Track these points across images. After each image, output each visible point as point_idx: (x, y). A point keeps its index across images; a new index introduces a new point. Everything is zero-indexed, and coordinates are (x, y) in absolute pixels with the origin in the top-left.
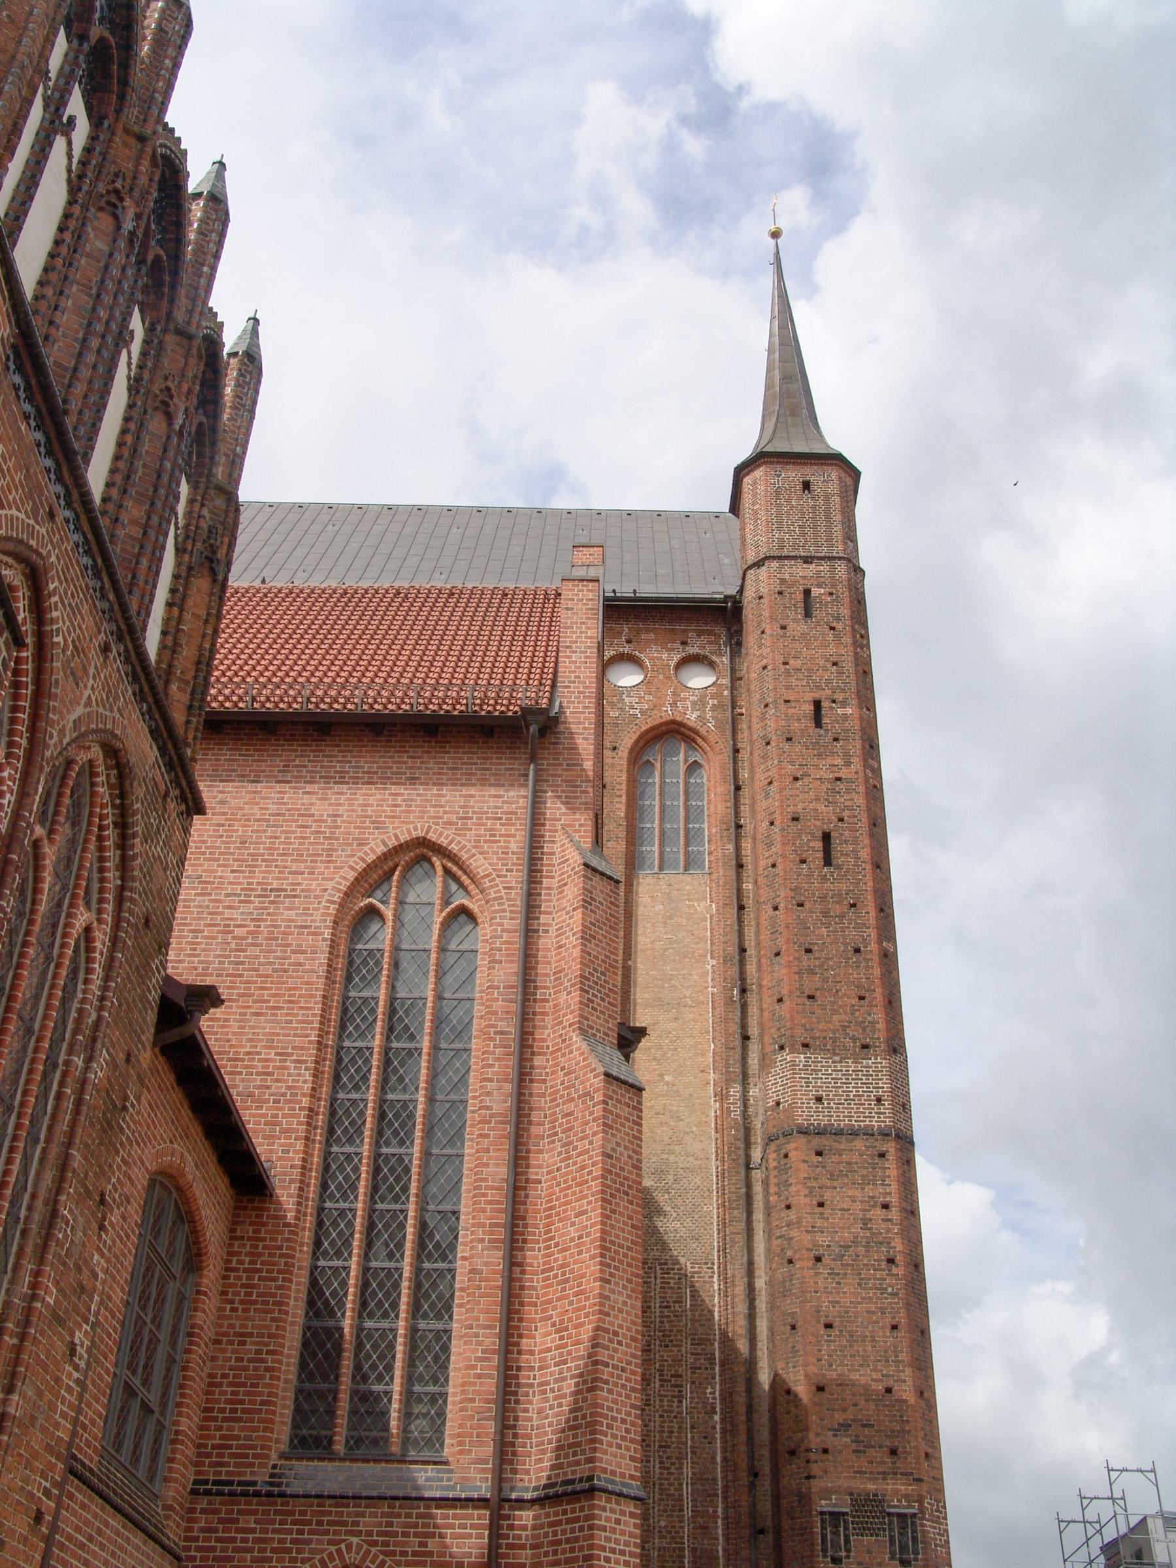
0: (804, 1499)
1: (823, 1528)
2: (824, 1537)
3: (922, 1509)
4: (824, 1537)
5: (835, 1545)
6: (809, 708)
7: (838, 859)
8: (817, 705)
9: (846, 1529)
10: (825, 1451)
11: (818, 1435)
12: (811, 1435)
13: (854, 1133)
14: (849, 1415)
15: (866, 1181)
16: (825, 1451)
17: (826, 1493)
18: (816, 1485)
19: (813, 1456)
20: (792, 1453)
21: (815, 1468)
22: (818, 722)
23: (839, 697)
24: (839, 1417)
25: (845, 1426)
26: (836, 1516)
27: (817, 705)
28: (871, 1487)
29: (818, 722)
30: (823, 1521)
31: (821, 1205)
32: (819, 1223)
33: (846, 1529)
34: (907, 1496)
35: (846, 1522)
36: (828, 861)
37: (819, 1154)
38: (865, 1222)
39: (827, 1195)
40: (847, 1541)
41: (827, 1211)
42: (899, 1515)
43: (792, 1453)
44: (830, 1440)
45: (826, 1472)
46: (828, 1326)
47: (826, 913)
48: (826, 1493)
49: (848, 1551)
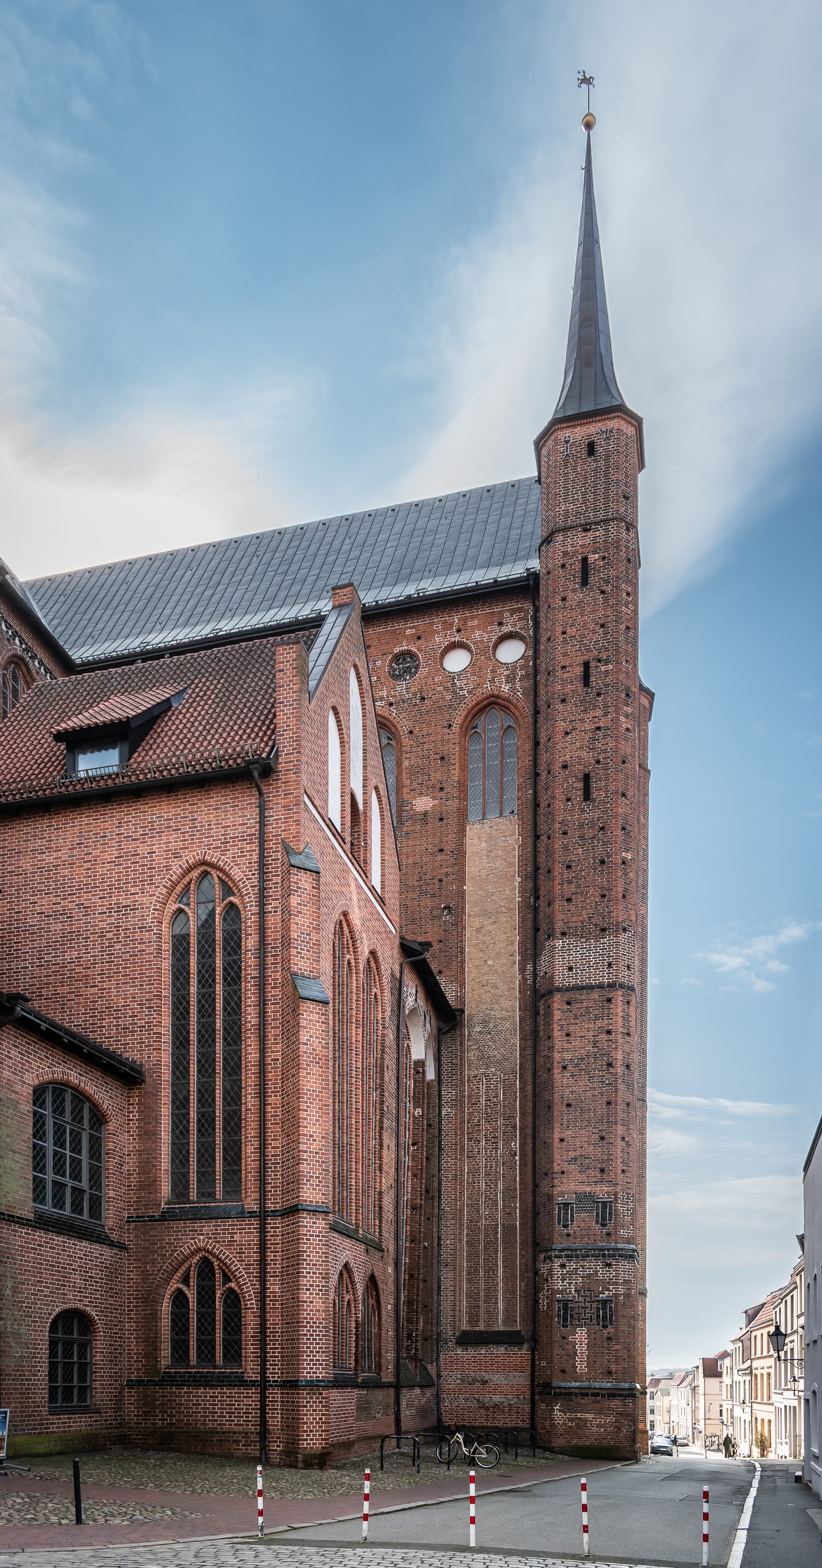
0: (550, 1197)
1: (559, 1211)
2: (559, 1215)
4: (559, 1215)
5: (566, 1219)
6: (579, 670)
9: (572, 1210)
10: (563, 1173)
11: (559, 1164)
12: (555, 1165)
13: (590, 988)
15: (597, 1018)
16: (563, 1173)
17: (562, 1194)
19: (556, 1176)
24: (572, 1154)
25: (575, 1159)
26: (566, 1205)
28: (588, 1189)
30: (559, 1208)
31: (568, 1035)
32: (566, 1046)
33: (572, 1210)
35: (572, 1208)
37: (569, 1003)
38: (595, 1043)
39: (572, 1028)
41: (571, 1038)
44: (565, 1167)
46: (569, 1105)
49: (572, 1221)
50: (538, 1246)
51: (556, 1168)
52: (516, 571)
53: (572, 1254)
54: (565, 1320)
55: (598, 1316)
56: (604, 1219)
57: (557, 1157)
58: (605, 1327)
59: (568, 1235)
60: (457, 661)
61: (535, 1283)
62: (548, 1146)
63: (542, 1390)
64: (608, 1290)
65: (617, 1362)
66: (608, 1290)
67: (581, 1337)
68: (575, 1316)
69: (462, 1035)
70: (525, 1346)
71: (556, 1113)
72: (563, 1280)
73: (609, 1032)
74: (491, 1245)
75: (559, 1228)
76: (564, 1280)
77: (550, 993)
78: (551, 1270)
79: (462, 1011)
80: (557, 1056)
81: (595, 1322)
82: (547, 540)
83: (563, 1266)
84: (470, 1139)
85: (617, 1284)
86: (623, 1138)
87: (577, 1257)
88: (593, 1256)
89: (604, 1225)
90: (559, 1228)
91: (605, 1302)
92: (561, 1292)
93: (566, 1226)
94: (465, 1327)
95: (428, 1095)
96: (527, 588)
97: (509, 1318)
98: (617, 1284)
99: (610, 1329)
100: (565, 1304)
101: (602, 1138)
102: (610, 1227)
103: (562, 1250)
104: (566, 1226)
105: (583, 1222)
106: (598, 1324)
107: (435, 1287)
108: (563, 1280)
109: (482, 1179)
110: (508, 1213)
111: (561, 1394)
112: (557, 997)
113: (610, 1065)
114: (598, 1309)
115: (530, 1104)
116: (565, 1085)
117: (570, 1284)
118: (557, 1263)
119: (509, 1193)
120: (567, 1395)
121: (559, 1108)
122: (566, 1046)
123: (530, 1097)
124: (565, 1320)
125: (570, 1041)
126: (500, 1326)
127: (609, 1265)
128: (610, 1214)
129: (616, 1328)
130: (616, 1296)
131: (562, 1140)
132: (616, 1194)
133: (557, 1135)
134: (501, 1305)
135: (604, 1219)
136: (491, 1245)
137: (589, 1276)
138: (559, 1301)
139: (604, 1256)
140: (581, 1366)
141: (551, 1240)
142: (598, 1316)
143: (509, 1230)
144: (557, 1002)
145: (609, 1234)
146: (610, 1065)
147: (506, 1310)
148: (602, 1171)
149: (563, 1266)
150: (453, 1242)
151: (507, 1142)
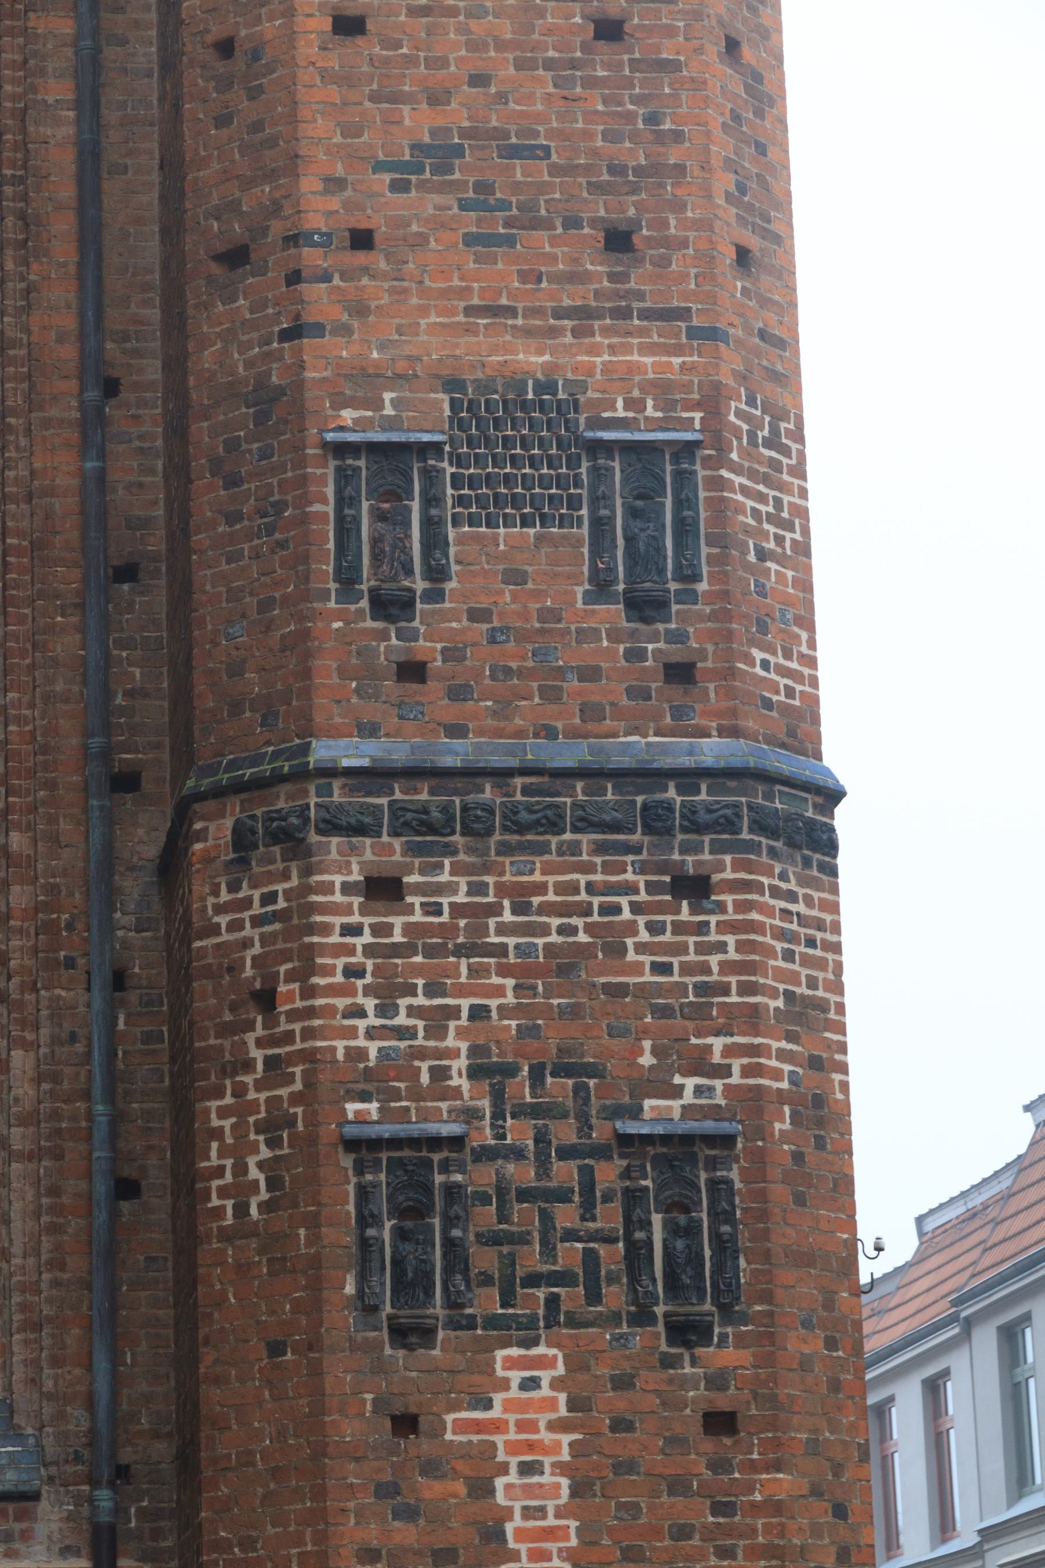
0: (276, 406)
1: (345, 501)
2: (346, 529)
3: (716, 432)
4: (346, 529)
5: (390, 554)
9: (431, 500)
11: (334, 184)
12: (309, 184)
14: (457, 115)
16: (362, 240)
17: (363, 385)
18: (320, 360)
19: (311, 257)
20: (236, 257)
21: (319, 300)
24: (417, 122)
25: (440, 154)
28: (533, 359)
30: (344, 477)
34: (663, 390)
35: (431, 477)
42: (629, 448)
43: (236, 257)
44: (384, 207)
45: (361, 311)
49: (437, 574)
51: (319, 210)
53: (441, 809)
54: (411, 1284)
55: (637, 1256)
56: (643, 558)
57: (319, 131)
58: (687, 1332)
59: (412, 671)
64: (699, 1064)
66: (699, 1064)
67: (522, 1412)
68: (484, 1259)
72: (388, 995)
75: (340, 620)
78: (297, 921)
81: (615, 1296)
83: (384, 889)
85: (752, 1018)
87: (476, 825)
88: (584, 823)
89: (645, 607)
90: (340, 620)
91: (677, 1150)
92: (372, 1082)
93: (392, 606)
98: (752, 1018)
99: (726, 1353)
100: (411, 1170)
102: (689, 624)
104: (392, 606)
106: (642, 1317)
108: (388, 995)
114: (633, 1198)
117: (438, 1020)
118: (341, 868)
124: (411, 1284)
127: (695, 888)
128: (685, 530)
129: (767, 1339)
130: (752, 1102)
132: (712, 402)
135: (643, 558)
137: (565, 964)
138: (362, 1148)
139: (656, 820)
141: (289, 709)
142: (637, 1256)
145: (681, 673)
148: (618, 241)
149: (384, 889)
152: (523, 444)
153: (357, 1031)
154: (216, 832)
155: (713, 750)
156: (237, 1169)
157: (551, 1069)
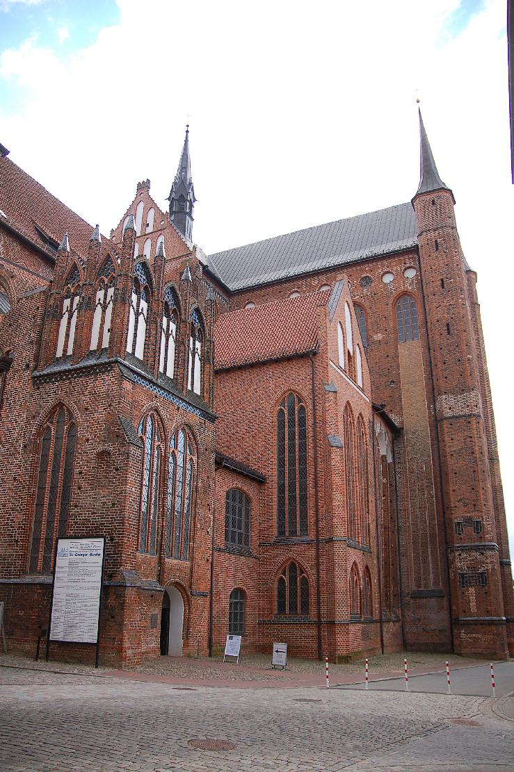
7: (451, 332)
8: (442, 280)
21: (453, 512)
22: (443, 287)
23: (449, 276)
24: (459, 498)
27: (442, 280)
29: (443, 287)
36: (449, 334)
40: (462, 529)
47: (449, 350)
48: (456, 518)
50: (448, 546)
52: (408, 243)
53: (464, 549)
55: (479, 581)
59: (461, 539)
60: (388, 279)
61: (448, 564)
62: (448, 494)
63: (455, 622)
65: (490, 605)
66: (483, 567)
69: (403, 440)
70: (445, 598)
71: (450, 477)
72: (460, 563)
73: (471, 437)
74: (425, 545)
76: (461, 563)
77: (442, 420)
79: (403, 428)
80: (448, 450)
82: (420, 235)
84: (411, 491)
85: (487, 563)
86: (483, 488)
87: (466, 550)
91: (482, 573)
94: (414, 588)
95: (389, 471)
96: (414, 250)
97: (436, 582)
98: (487, 563)
99: (486, 588)
101: (473, 489)
102: (481, 534)
103: (459, 547)
105: (469, 530)
107: (398, 566)
108: (460, 563)
109: (417, 508)
110: (433, 528)
111: (464, 624)
112: (445, 421)
113: (473, 453)
115: (438, 472)
116: (453, 463)
119: (432, 517)
120: (468, 623)
121: (451, 475)
122: (451, 444)
123: (438, 468)
125: (452, 444)
126: (431, 587)
129: (489, 587)
131: (454, 491)
132: (482, 517)
133: (451, 489)
134: (431, 576)
135: (478, 529)
136: (425, 545)
138: (460, 574)
140: (473, 609)
142: (479, 581)
143: (433, 536)
144: (446, 424)
146: (473, 453)
147: (434, 579)
148: (475, 505)
150: (406, 540)
151: (429, 491)
152: (469, 521)
153: (459, 565)
154: (449, 551)
155: (483, 544)
156: (452, 575)
157: (473, 568)
